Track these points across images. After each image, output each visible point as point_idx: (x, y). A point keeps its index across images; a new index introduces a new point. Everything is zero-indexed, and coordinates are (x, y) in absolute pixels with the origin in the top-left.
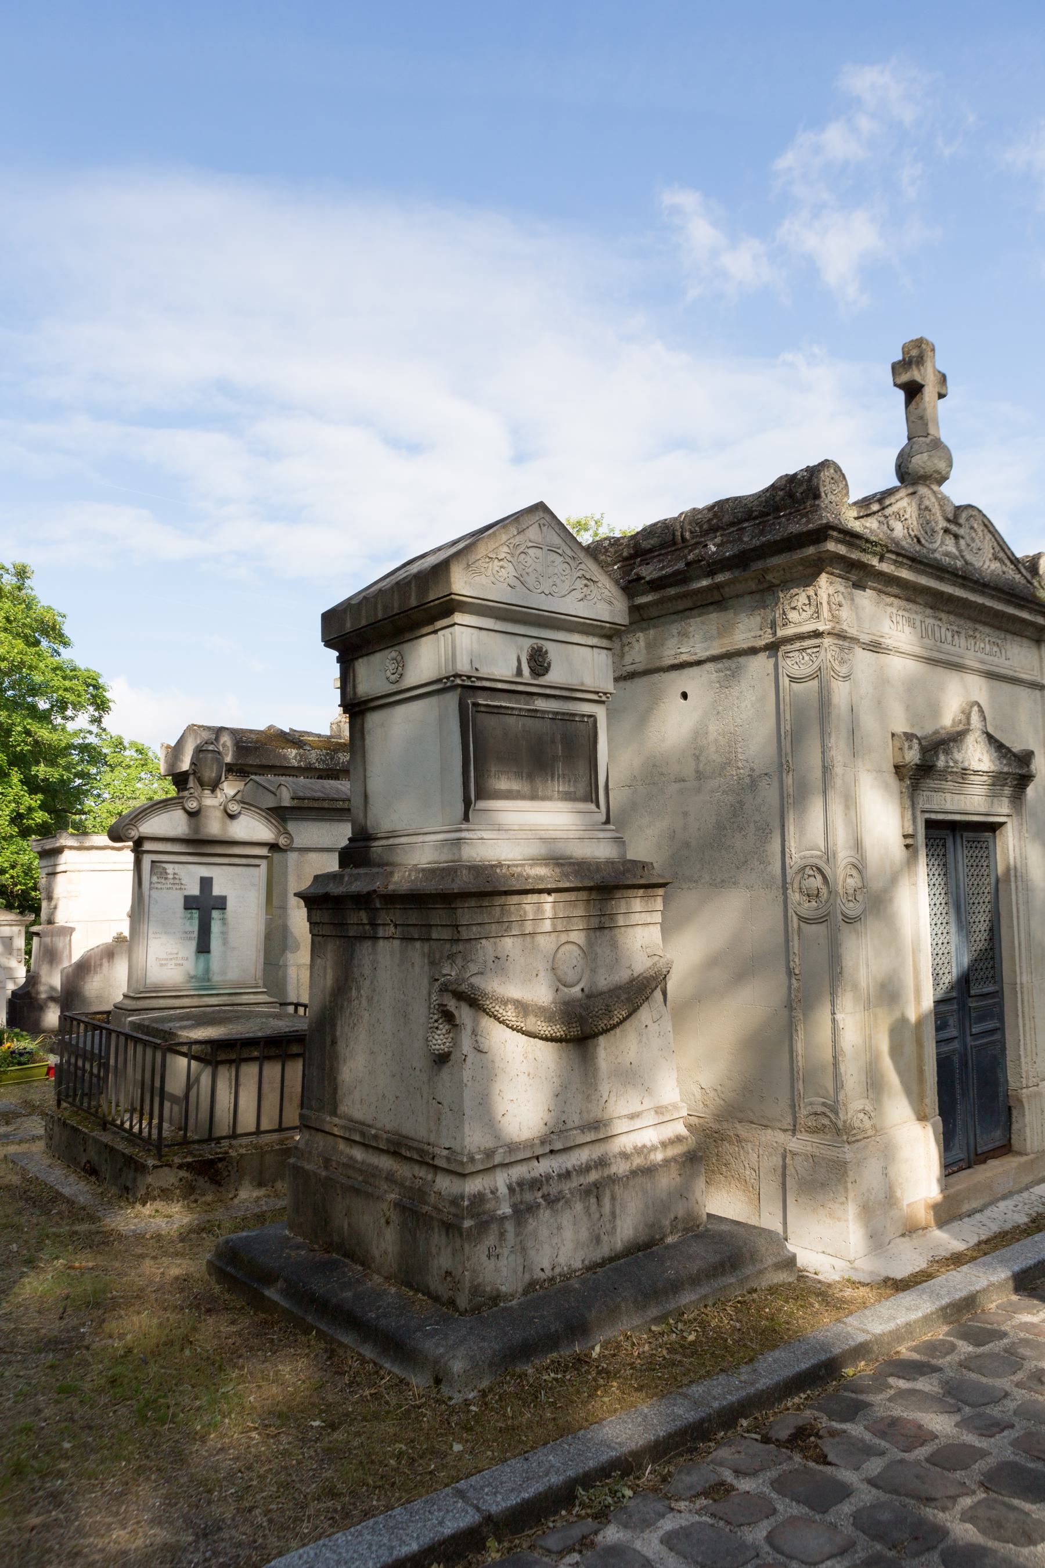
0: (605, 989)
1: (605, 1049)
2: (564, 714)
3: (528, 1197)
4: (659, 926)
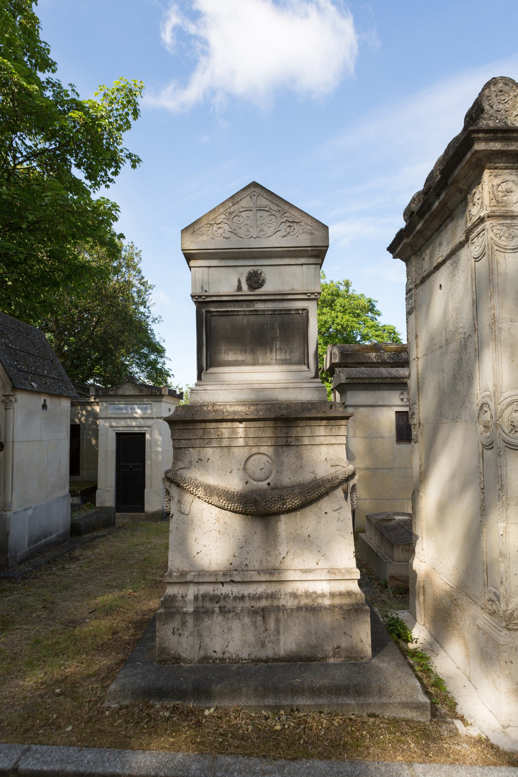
0: (289, 485)
1: (285, 524)
2: (280, 310)
3: (208, 605)
4: (344, 445)
